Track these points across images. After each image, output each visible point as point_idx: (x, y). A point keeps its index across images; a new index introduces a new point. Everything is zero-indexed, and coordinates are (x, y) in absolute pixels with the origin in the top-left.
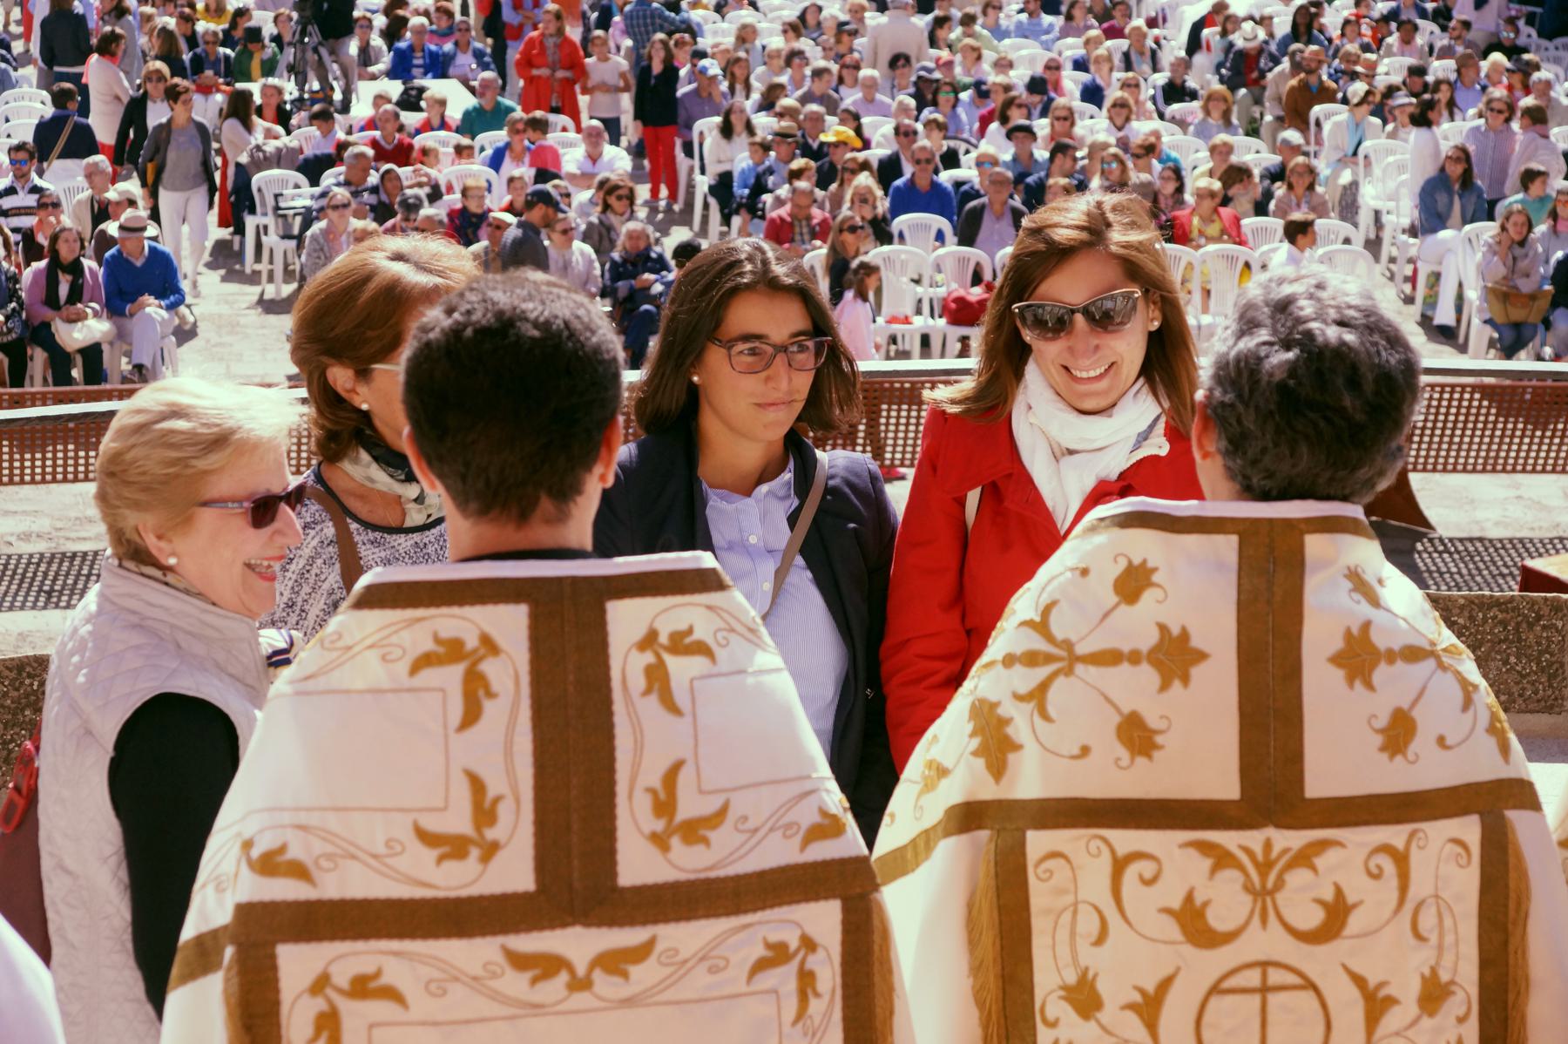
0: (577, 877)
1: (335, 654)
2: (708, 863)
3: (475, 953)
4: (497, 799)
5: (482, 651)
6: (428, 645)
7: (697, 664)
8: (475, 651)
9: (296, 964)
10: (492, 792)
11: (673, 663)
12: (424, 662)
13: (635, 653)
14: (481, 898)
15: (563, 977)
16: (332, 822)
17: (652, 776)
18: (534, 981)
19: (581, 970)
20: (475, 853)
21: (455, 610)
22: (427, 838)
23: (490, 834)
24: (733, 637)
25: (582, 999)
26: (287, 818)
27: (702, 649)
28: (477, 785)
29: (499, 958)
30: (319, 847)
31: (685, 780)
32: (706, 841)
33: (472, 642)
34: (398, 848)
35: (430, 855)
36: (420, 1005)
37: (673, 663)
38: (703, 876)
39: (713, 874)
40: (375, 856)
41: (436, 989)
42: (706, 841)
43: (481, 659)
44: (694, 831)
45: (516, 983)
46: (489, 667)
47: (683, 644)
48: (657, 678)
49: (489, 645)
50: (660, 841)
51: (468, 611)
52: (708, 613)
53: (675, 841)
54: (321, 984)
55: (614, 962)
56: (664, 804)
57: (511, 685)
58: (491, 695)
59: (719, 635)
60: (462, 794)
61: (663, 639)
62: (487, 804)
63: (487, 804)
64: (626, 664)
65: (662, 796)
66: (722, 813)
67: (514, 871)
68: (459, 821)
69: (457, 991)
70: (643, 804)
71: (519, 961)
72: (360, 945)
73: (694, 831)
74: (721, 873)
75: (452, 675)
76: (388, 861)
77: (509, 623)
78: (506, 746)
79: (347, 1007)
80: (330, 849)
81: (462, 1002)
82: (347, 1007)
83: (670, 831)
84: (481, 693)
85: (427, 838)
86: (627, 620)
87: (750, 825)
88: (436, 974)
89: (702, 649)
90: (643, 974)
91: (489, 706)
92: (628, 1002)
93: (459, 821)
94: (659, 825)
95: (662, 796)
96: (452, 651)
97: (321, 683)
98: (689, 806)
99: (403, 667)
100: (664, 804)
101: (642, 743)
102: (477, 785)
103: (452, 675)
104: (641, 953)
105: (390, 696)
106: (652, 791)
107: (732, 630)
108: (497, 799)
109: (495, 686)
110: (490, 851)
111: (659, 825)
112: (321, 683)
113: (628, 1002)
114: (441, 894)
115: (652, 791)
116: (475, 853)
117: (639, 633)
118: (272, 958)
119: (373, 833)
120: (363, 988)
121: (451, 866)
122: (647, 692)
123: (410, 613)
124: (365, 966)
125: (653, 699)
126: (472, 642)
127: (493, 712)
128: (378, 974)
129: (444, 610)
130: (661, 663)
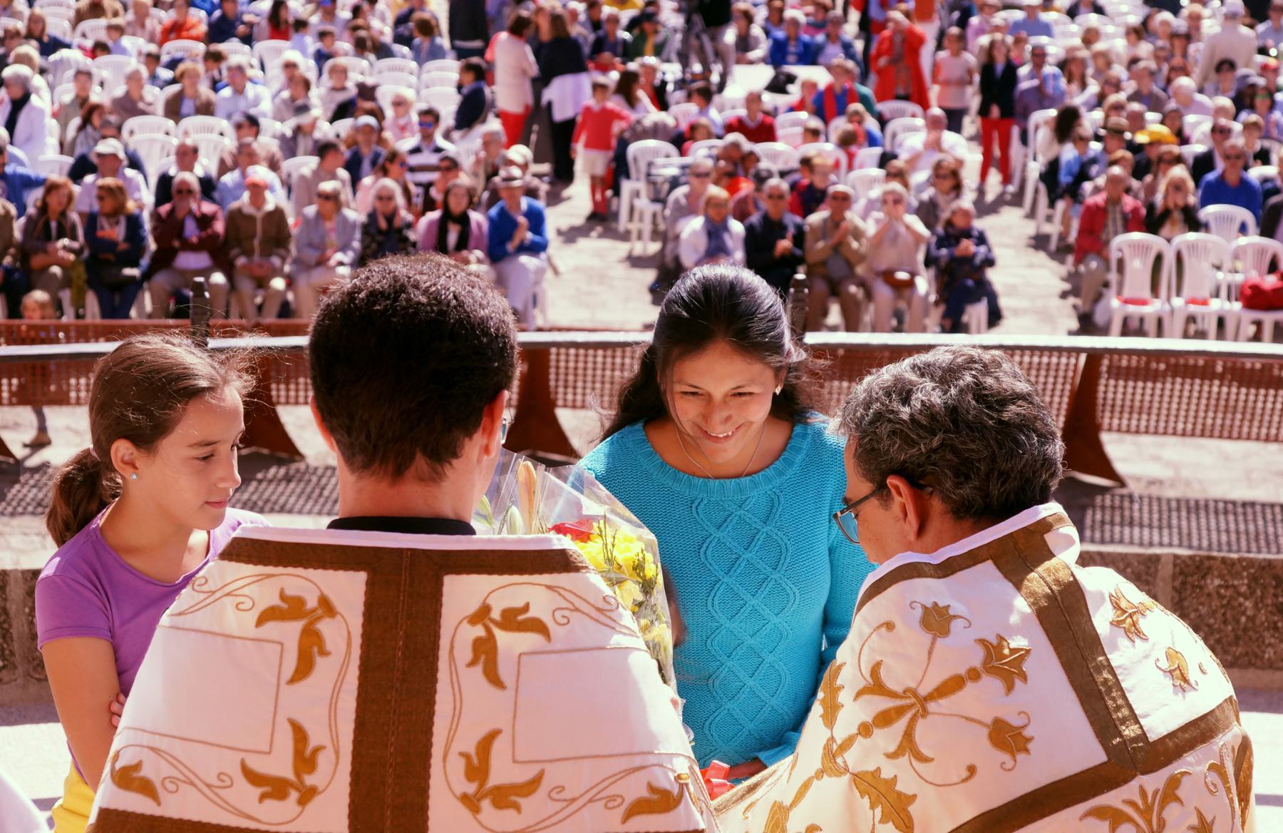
5: (320, 612)
8: (314, 611)
12: (267, 616)
33: (312, 602)
43: (319, 619)
46: (326, 627)
51: (310, 573)
58: (324, 653)
62: (308, 752)
63: (308, 752)
75: (291, 631)
91: (320, 662)
103: (291, 631)
109: (329, 646)
126: (312, 602)
127: (325, 669)
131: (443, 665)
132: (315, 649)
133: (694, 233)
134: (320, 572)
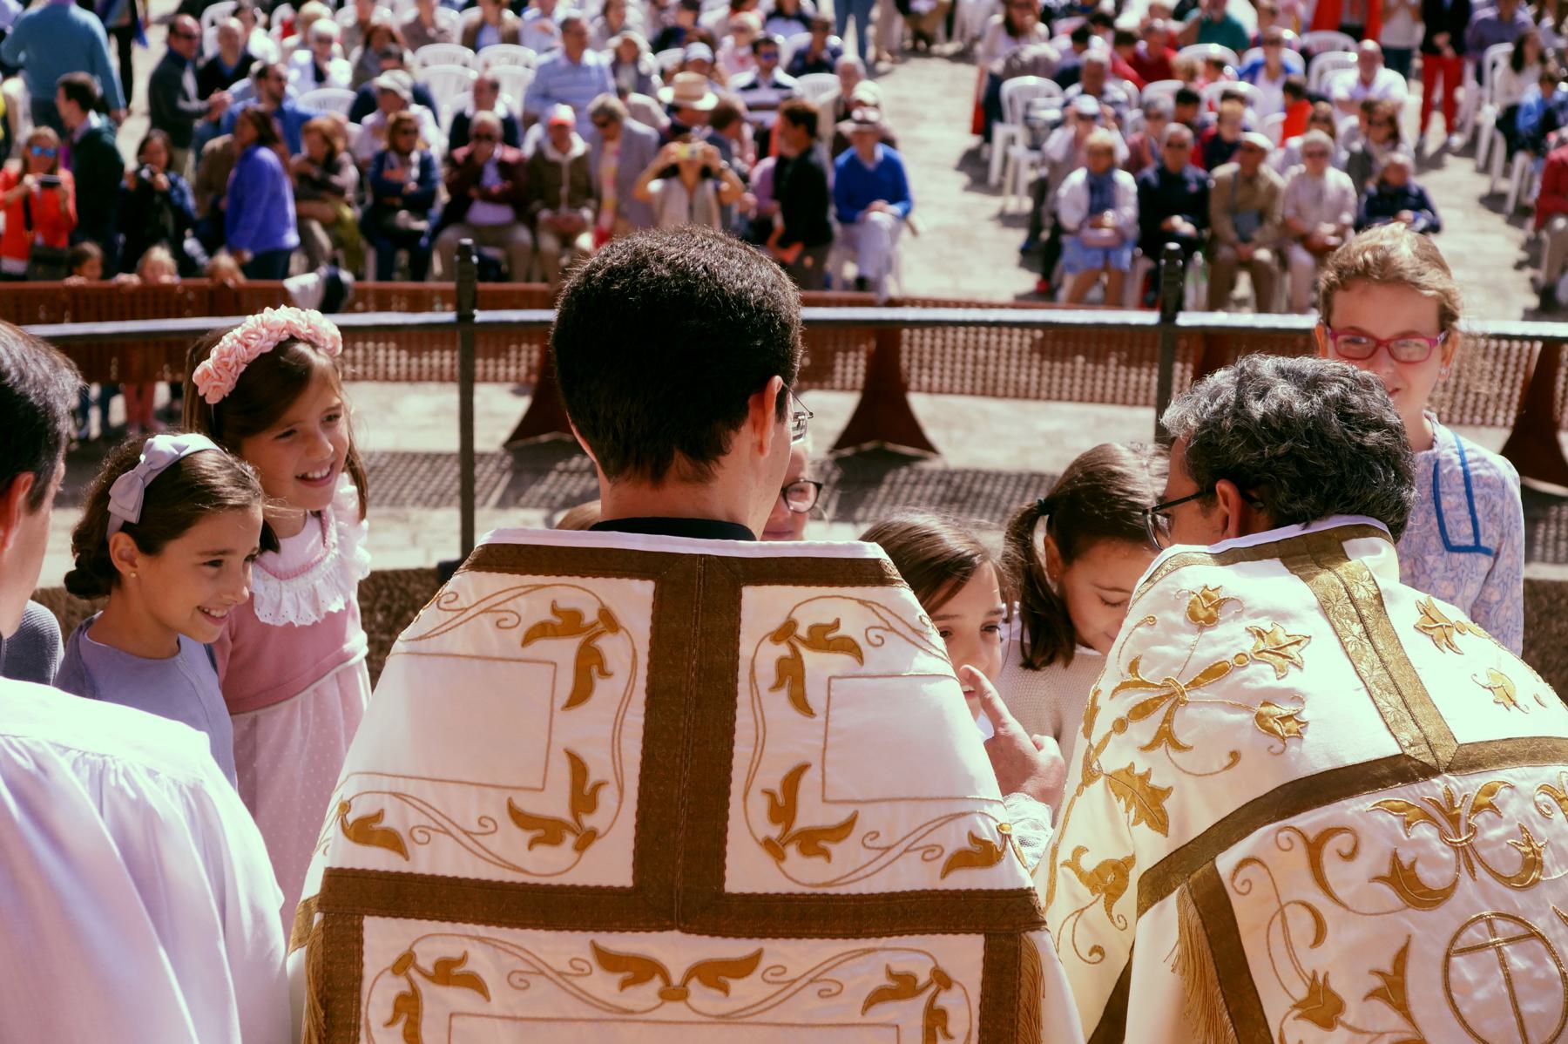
0: (679, 877)
1: (450, 615)
2: (828, 879)
3: (563, 948)
4: (598, 786)
5: (600, 626)
6: (546, 615)
7: (839, 662)
8: (593, 625)
9: (383, 938)
10: (593, 777)
11: (812, 660)
12: (540, 631)
13: (767, 644)
14: (574, 888)
15: (657, 983)
16: (429, 793)
17: (772, 778)
18: (624, 985)
19: (676, 979)
20: (570, 839)
21: (577, 580)
22: (520, 818)
23: (589, 821)
24: (891, 638)
25: (675, 1010)
26: (386, 783)
27: (848, 646)
28: (578, 767)
29: (589, 956)
30: (414, 818)
31: (809, 781)
32: (827, 855)
33: (590, 616)
34: (491, 827)
35: (522, 837)
36: (501, 998)
37: (812, 660)
38: (820, 891)
39: (831, 891)
40: (466, 833)
41: (516, 983)
42: (827, 855)
43: (599, 634)
44: (813, 842)
45: (604, 985)
46: (610, 646)
47: (825, 638)
48: (790, 674)
49: (608, 621)
50: (774, 848)
52: (862, 608)
53: (792, 851)
54: (404, 963)
55: (714, 974)
56: (783, 808)
57: (628, 662)
58: (604, 673)
59: (872, 634)
60: (561, 774)
61: (802, 631)
64: (757, 653)
65: (781, 800)
66: (847, 827)
67: (611, 863)
68: (556, 804)
69: (541, 986)
70: (759, 805)
71: (609, 962)
72: (447, 927)
73: (813, 842)
74: (843, 890)
75: (565, 650)
76: (479, 839)
77: (633, 600)
78: (613, 729)
79: (427, 989)
80: (424, 821)
81: (544, 998)
82: (427, 989)
83: (785, 840)
84: (595, 670)
85: (520, 818)
86: (762, 607)
87: (882, 842)
88: (522, 967)
89: (848, 646)
90: (744, 990)
91: (601, 685)
92: (725, 1019)
93: (556, 804)
94: (775, 832)
95: (781, 800)
96: (567, 623)
97: (433, 645)
98: (811, 814)
99: (517, 635)
100: (783, 808)
101: (765, 737)
102: (578, 767)
103: (565, 650)
104: (744, 967)
105: (500, 664)
106: (770, 794)
107: (892, 629)
108: (598, 786)
109: (611, 666)
110: (587, 839)
111: (775, 832)
112: (433, 645)
113: (725, 1019)
114: (531, 880)
115: (770, 794)
116: (570, 839)
117: (776, 622)
118: (359, 928)
119: (467, 808)
120: (448, 972)
121: (542, 851)
122: (777, 687)
123: (529, 579)
124: (452, 950)
125: (783, 694)
126: (590, 616)
127: (606, 691)
128: (464, 959)
129: (564, 579)
130: (797, 655)
131: (743, 697)
132: (595, 670)
133: (1073, 189)
134: (601, 580)
